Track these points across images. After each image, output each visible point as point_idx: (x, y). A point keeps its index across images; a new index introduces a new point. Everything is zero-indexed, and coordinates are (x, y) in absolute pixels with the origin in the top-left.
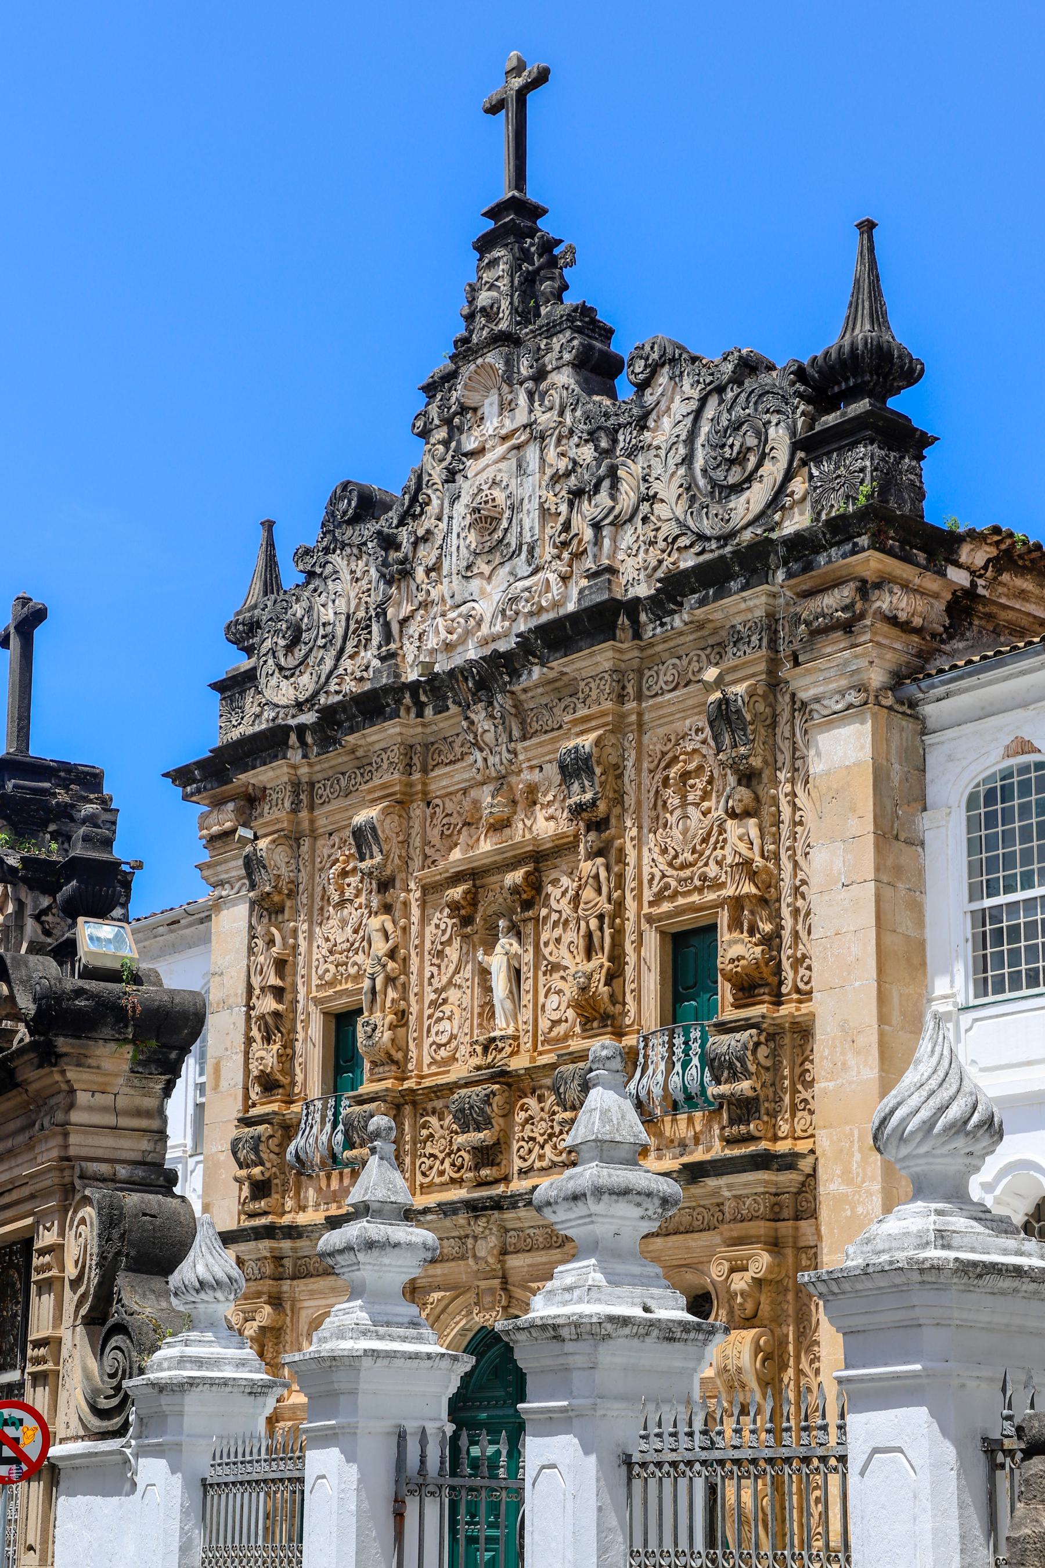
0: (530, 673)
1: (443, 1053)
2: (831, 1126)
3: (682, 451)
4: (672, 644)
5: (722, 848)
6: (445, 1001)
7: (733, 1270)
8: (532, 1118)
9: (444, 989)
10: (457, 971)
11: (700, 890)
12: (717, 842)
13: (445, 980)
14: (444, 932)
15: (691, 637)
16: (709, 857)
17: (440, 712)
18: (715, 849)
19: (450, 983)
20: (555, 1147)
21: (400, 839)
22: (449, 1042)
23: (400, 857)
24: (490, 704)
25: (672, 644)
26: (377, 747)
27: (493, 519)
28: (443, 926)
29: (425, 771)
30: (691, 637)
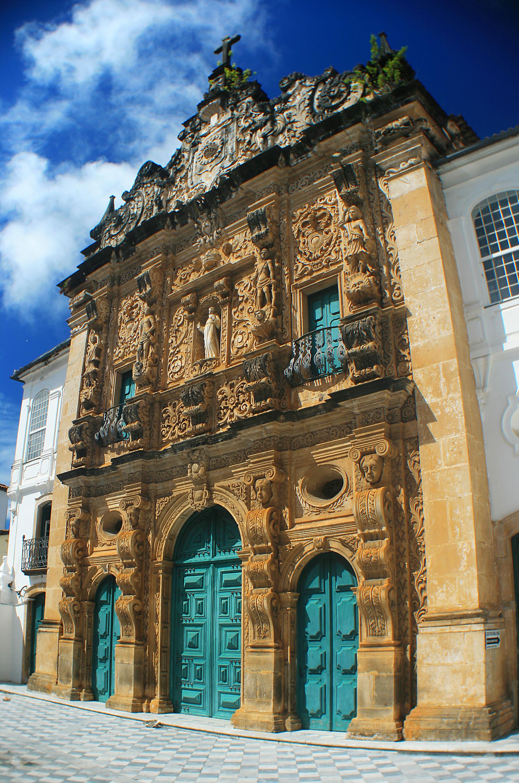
0: (230, 197)
1: (176, 376)
2: (423, 366)
3: (307, 102)
4: (305, 168)
5: (339, 245)
6: (179, 352)
7: (363, 454)
8: (226, 397)
9: (178, 346)
10: (185, 337)
11: (327, 267)
12: (336, 243)
13: (178, 342)
14: (180, 320)
15: (316, 163)
16: (331, 251)
17: (184, 225)
18: (334, 246)
19: (181, 343)
20: (240, 410)
21: (160, 283)
22: (180, 370)
23: (159, 291)
24: (209, 213)
25: (305, 168)
26: (152, 249)
27: (214, 149)
28: (179, 318)
29: (174, 254)
30: (316, 163)
